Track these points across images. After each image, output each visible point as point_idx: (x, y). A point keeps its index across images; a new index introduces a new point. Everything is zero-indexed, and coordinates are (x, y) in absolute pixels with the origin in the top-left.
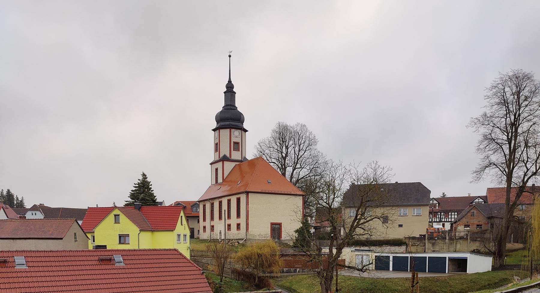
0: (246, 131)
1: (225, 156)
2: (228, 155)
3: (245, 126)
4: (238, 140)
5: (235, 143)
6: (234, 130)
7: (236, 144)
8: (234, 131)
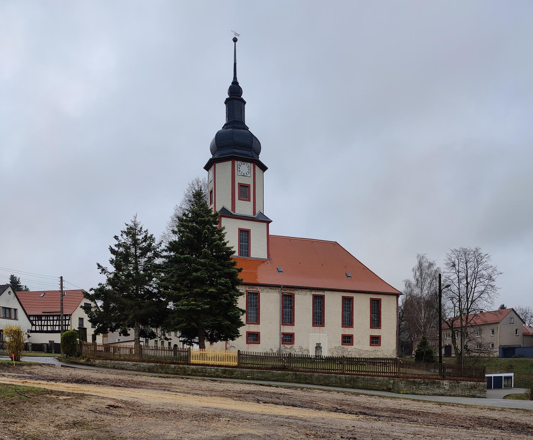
0: (264, 168)
1: (224, 209)
2: (229, 208)
3: (262, 158)
4: (248, 181)
5: (241, 185)
6: (239, 162)
7: (244, 187)
8: (241, 164)
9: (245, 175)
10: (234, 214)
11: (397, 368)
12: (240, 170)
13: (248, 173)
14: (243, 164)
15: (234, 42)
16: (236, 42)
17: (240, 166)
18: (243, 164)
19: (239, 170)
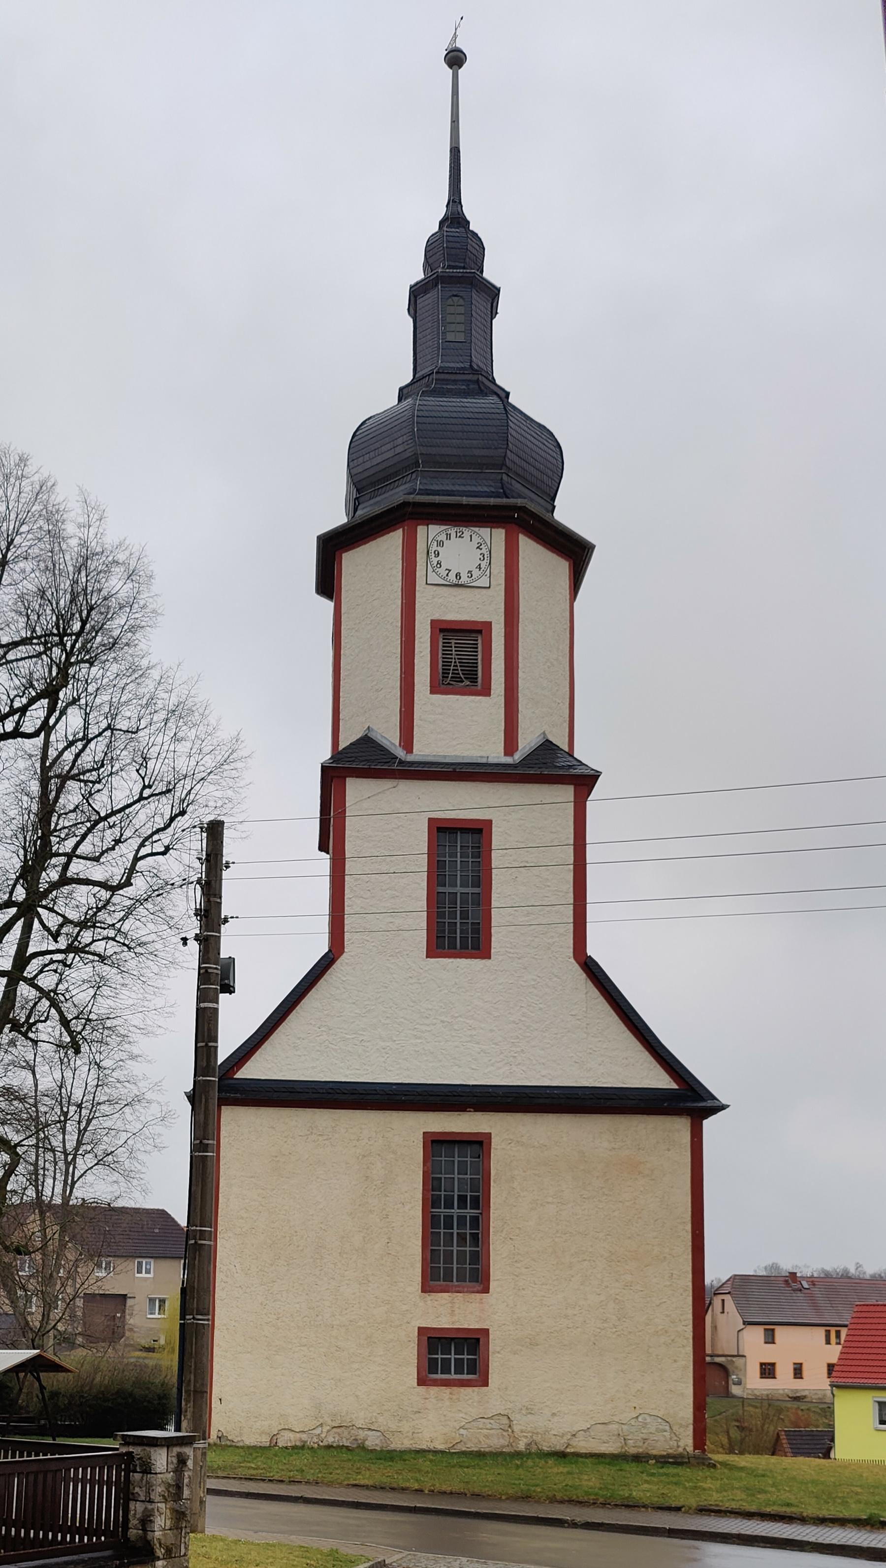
1: (367, 743)
6: (434, 530)
8: (443, 537)
9: (464, 579)
10: (410, 758)
11: (186, 1271)
12: (439, 563)
13: (476, 572)
14: (453, 535)
15: (451, 66)
16: (460, 67)
17: (440, 544)
18: (453, 535)
19: (435, 561)
